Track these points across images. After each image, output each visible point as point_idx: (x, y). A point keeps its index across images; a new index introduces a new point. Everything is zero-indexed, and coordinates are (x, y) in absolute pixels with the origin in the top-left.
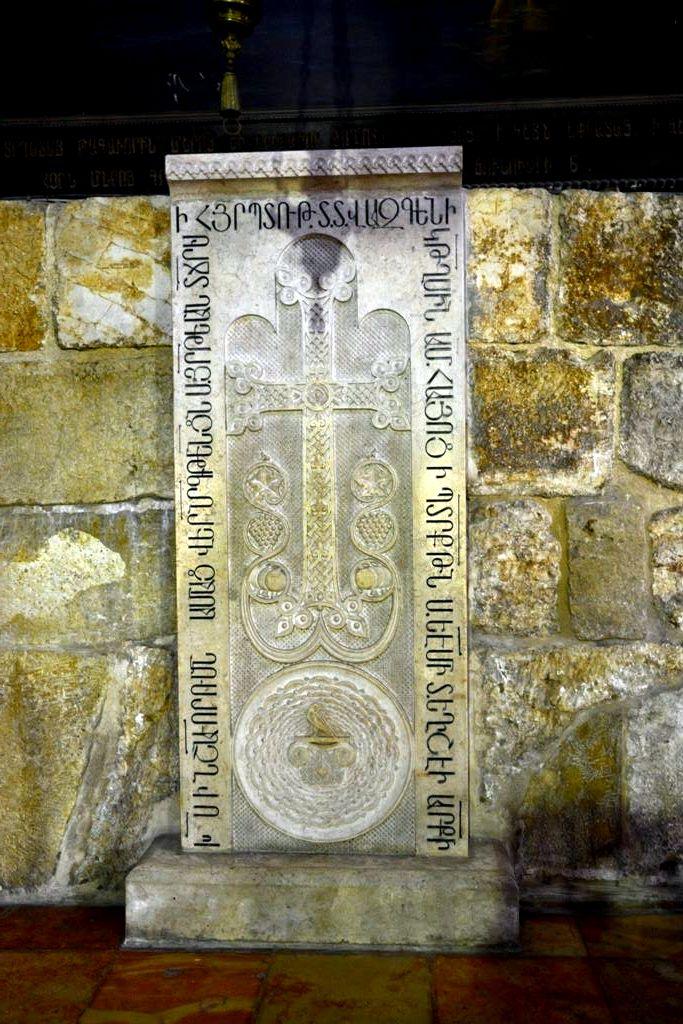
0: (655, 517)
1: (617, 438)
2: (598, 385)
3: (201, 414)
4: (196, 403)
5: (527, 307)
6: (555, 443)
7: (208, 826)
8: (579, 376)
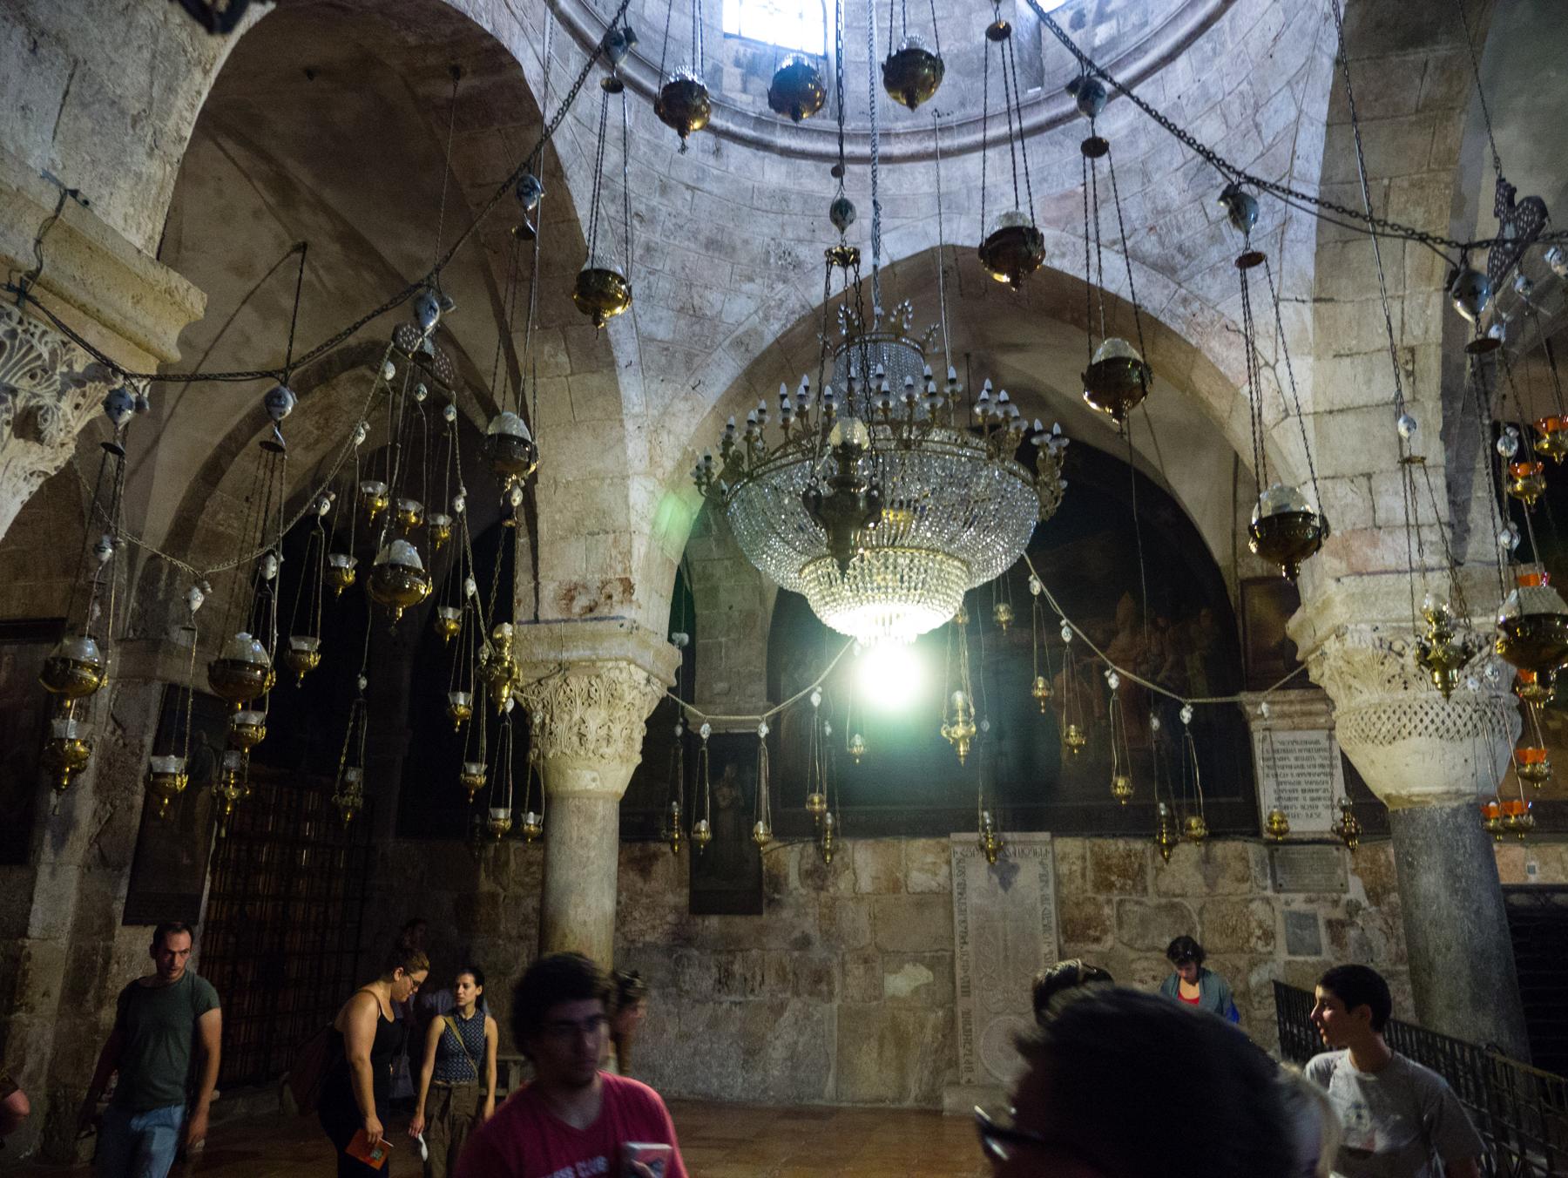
0: (1133, 961)
1: (1116, 930)
2: (1107, 911)
3: (964, 921)
4: (962, 918)
5: (1079, 881)
6: (1091, 932)
7: (969, 1075)
8: (1099, 907)
